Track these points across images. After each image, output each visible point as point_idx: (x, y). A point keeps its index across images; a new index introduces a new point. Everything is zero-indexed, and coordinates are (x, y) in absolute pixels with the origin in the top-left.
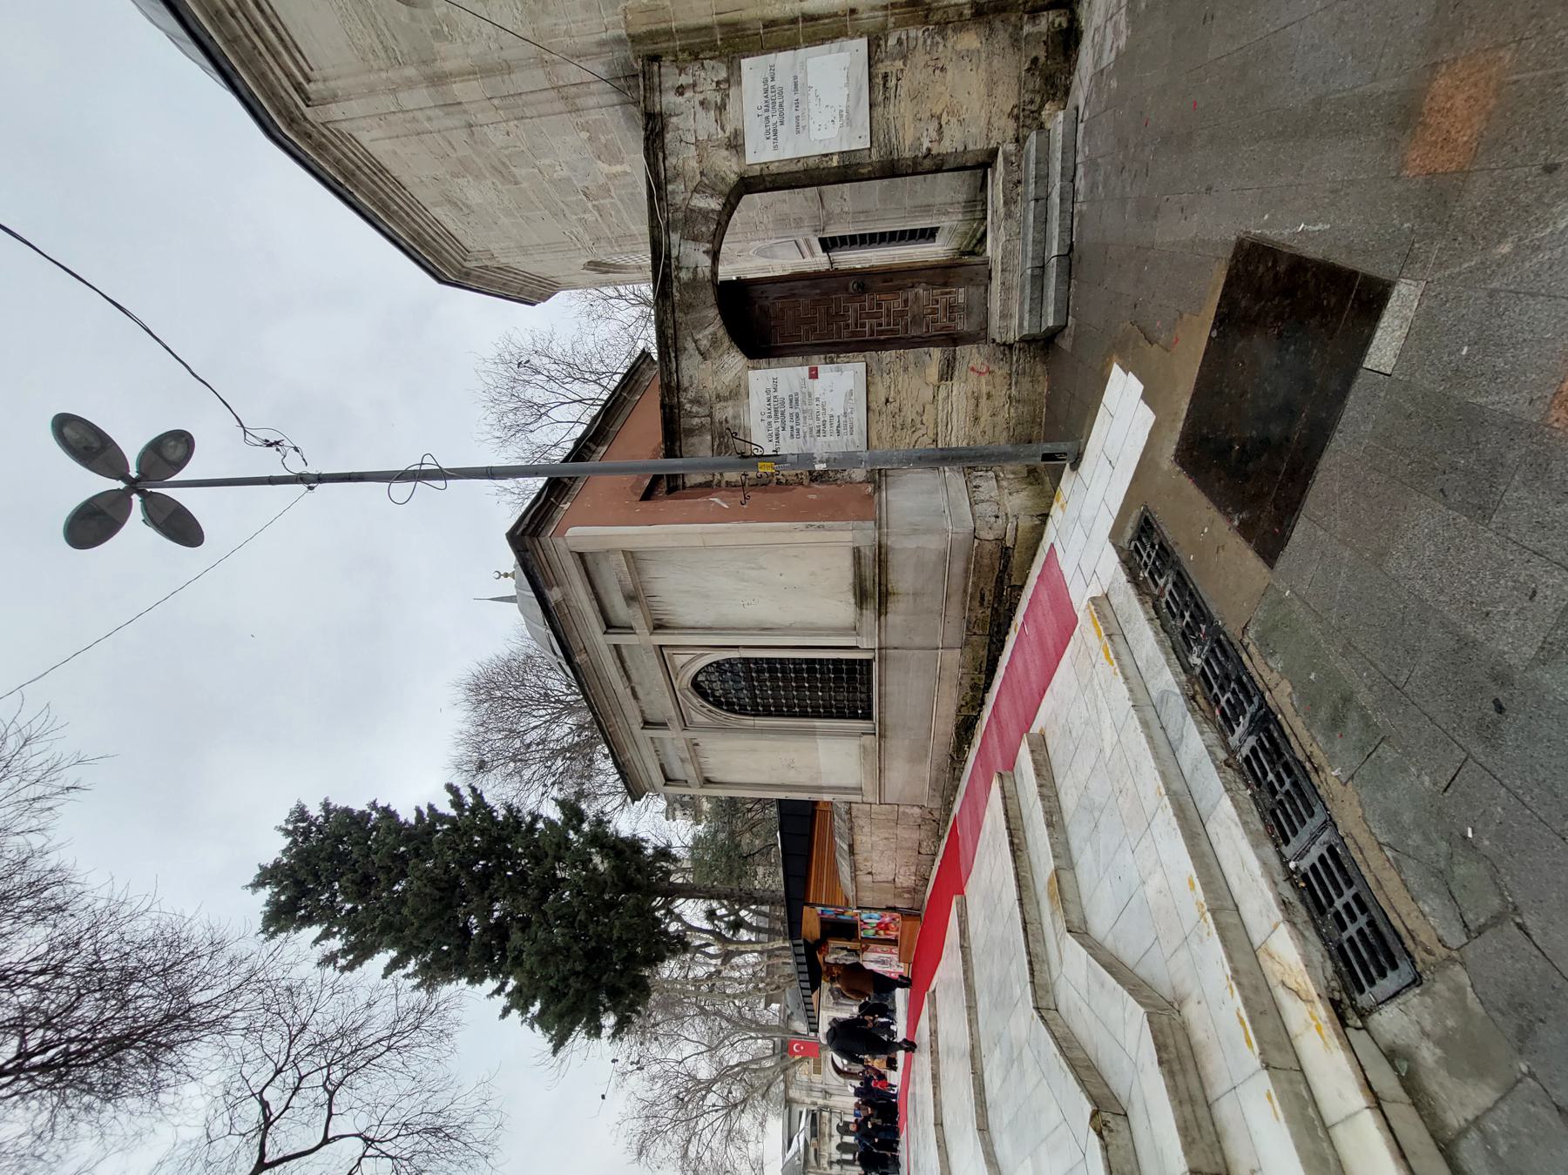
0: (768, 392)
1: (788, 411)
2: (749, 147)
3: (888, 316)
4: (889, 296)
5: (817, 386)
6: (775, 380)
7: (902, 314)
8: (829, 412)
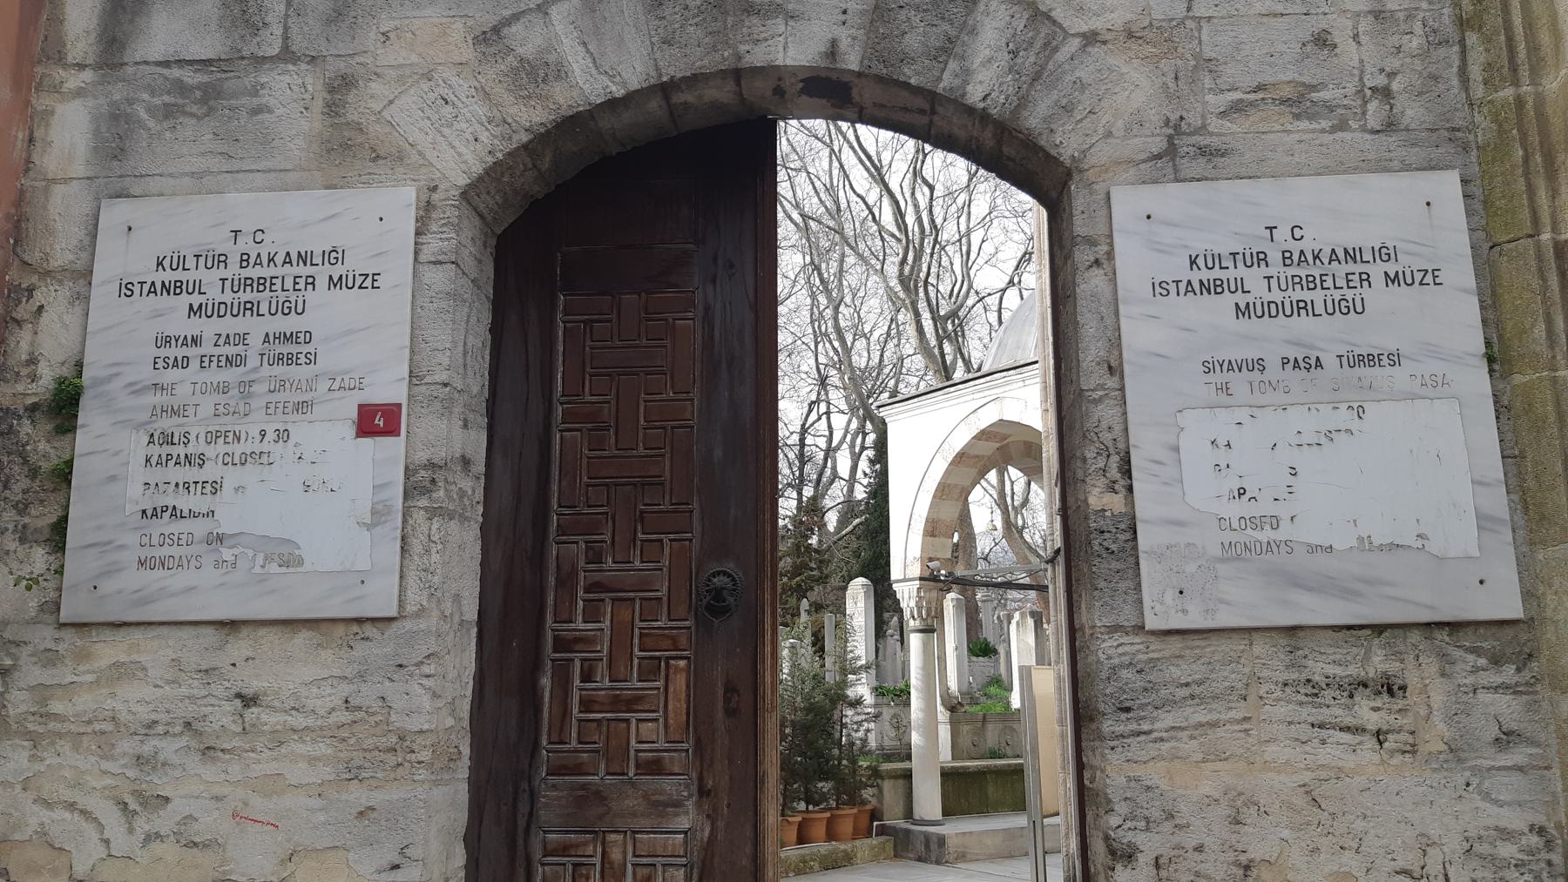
0: (334, 255)
1: (256, 328)
2: (1171, 199)
3: (616, 703)
4: (678, 706)
5: (329, 436)
6: (369, 281)
7: (616, 755)
8: (232, 477)
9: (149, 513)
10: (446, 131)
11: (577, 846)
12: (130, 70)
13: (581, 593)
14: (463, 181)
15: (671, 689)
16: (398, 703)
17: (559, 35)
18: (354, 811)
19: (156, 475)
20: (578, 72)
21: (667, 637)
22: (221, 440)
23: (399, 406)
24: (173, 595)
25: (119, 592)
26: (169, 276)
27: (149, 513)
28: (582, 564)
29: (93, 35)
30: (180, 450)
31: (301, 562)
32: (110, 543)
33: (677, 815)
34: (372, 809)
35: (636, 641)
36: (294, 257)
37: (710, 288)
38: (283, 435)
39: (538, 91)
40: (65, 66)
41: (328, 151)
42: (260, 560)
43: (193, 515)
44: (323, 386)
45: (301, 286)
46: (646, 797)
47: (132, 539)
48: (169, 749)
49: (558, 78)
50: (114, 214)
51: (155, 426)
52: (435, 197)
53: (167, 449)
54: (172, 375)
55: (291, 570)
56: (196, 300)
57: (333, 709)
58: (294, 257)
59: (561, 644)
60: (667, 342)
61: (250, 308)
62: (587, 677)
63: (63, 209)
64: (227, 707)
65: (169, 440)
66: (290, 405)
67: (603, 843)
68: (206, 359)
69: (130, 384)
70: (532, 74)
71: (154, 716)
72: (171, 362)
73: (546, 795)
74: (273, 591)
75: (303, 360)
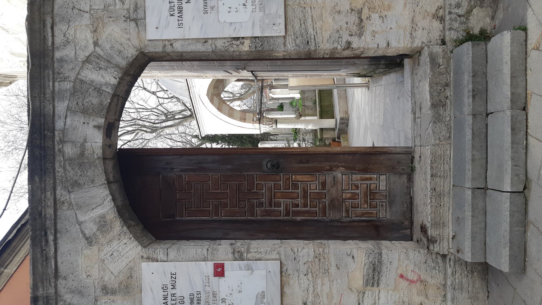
0: (164, 288)
2: (151, 21)
3: (305, 196)
4: (306, 178)
5: (223, 286)
6: (173, 276)
7: (320, 196)
10: (122, 254)
13: (272, 209)
14: (140, 247)
15: (301, 180)
16: (306, 259)
18: (337, 270)
20: (103, 211)
23: (214, 264)
28: (263, 209)
31: (263, 292)
33: (337, 178)
34: (337, 265)
35: (287, 191)
36: (165, 301)
37: (175, 170)
44: (208, 289)
45: (174, 298)
49: (105, 217)
52: (145, 256)
58: (165, 301)
59: (288, 214)
62: (297, 206)
67: (346, 199)
75: (199, 296)
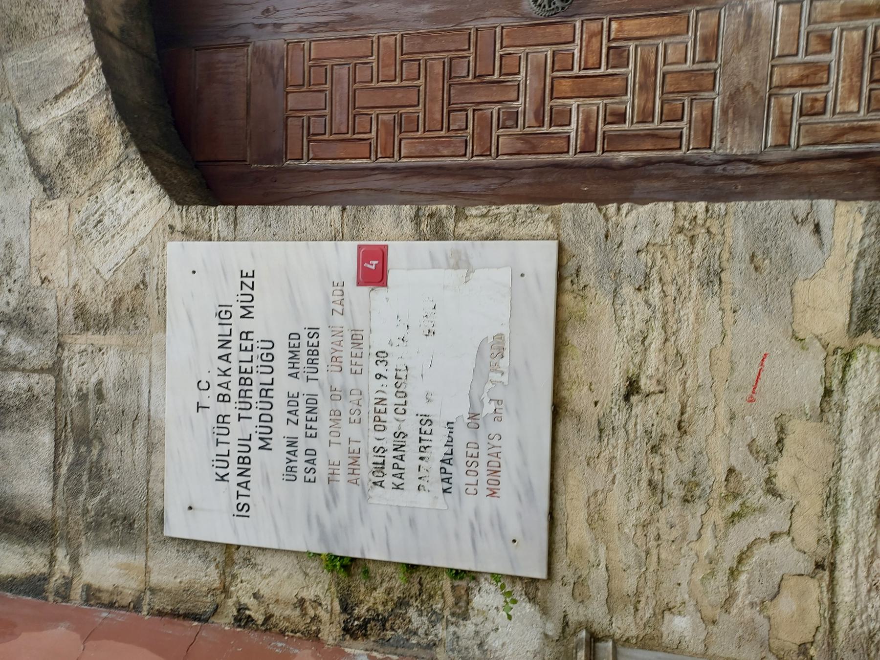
0: (223, 315)
1: (284, 385)
3: (647, 87)
4: (651, 26)
5: (381, 313)
6: (247, 279)
7: (697, 82)
8: (417, 406)
9: (446, 486)
10: (124, 220)
11: (782, 113)
12: (59, 513)
13: (545, 129)
14: (166, 201)
15: (638, 34)
16: (645, 235)
17: (50, 124)
18: (754, 275)
19: (411, 478)
20: (79, 102)
21: (589, 42)
22: (383, 417)
23: (360, 247)
24: (525, 463)
25: (519, 515)
26: (234, 469)
27: (446, 486)
28: (517, 131)
29: (29, 549)
30: (390, 455)
31: (500, 337)
32: (472, 526)
33: (759, 15)
34: (753, 257)
35: (590, 72)
36: (223, 352)
37: (285, 29)
38: (381, 357)
39: (94, 138)
40: (51, 574)
41: (137, 328)
42: (495, 376)
43: (450, 443)
44: (338, 320)
45: (248, 344)
46: (739, 49)
47: (469, 502)
48: (673, 477)
49: (84, 120)
50: (177, 525)
51: (366, 480)
52: (179, 227)
53: (388, 469)
54: (321, 466)
55: (507, 346)
56: (256, 443)
57: (646, 302)
58: (223, 352)
59: (588, 147)
60: (329, 63)
61: (266, 391)
62: (621, 117)
63: (171, 572)
64: (637, 410)
65: (380, 467)
66: (354, 351)
67: (781, 87)
68: (309, 432)
69: (328, 505)
70: (81, 144)
71: (644, 484)
72: (310, 466)
73: (731, 148)
74: (526, 363)
75: (314, 341)
